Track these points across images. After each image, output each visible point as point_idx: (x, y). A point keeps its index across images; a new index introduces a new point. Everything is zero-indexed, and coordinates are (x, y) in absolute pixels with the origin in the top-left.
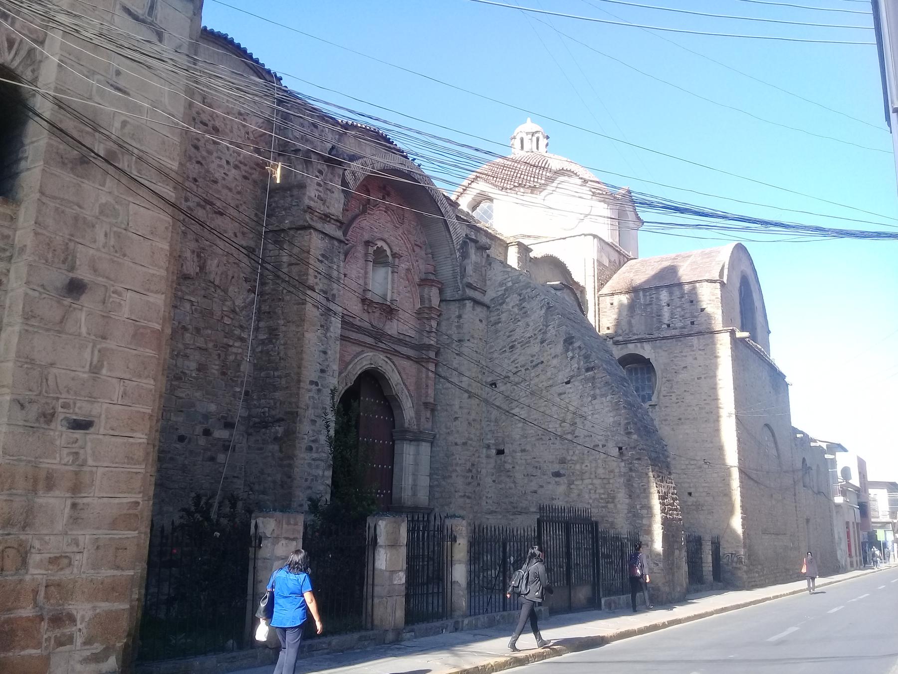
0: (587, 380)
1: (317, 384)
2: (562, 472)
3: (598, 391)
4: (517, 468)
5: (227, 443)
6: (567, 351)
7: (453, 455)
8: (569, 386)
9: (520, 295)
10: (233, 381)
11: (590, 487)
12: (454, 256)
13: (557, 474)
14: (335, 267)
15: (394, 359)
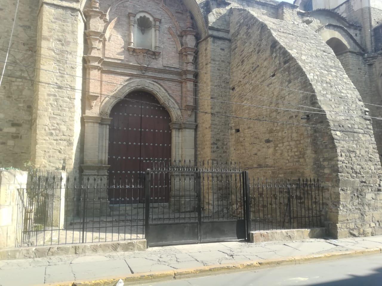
0: (285, 70)
1: (55, 96)
2: (271, 139)
3: (292, 76)
4: (246, 140)
5: (15, 135)
6: (272, 53)
7: (205, 135)
8: (274, 77)
9: (247, 26)
10: (17, 101)
11: (288, 147)
12: (200, 12)
13: (268, 141)
14: (69, 24)
15: (161, 82)
